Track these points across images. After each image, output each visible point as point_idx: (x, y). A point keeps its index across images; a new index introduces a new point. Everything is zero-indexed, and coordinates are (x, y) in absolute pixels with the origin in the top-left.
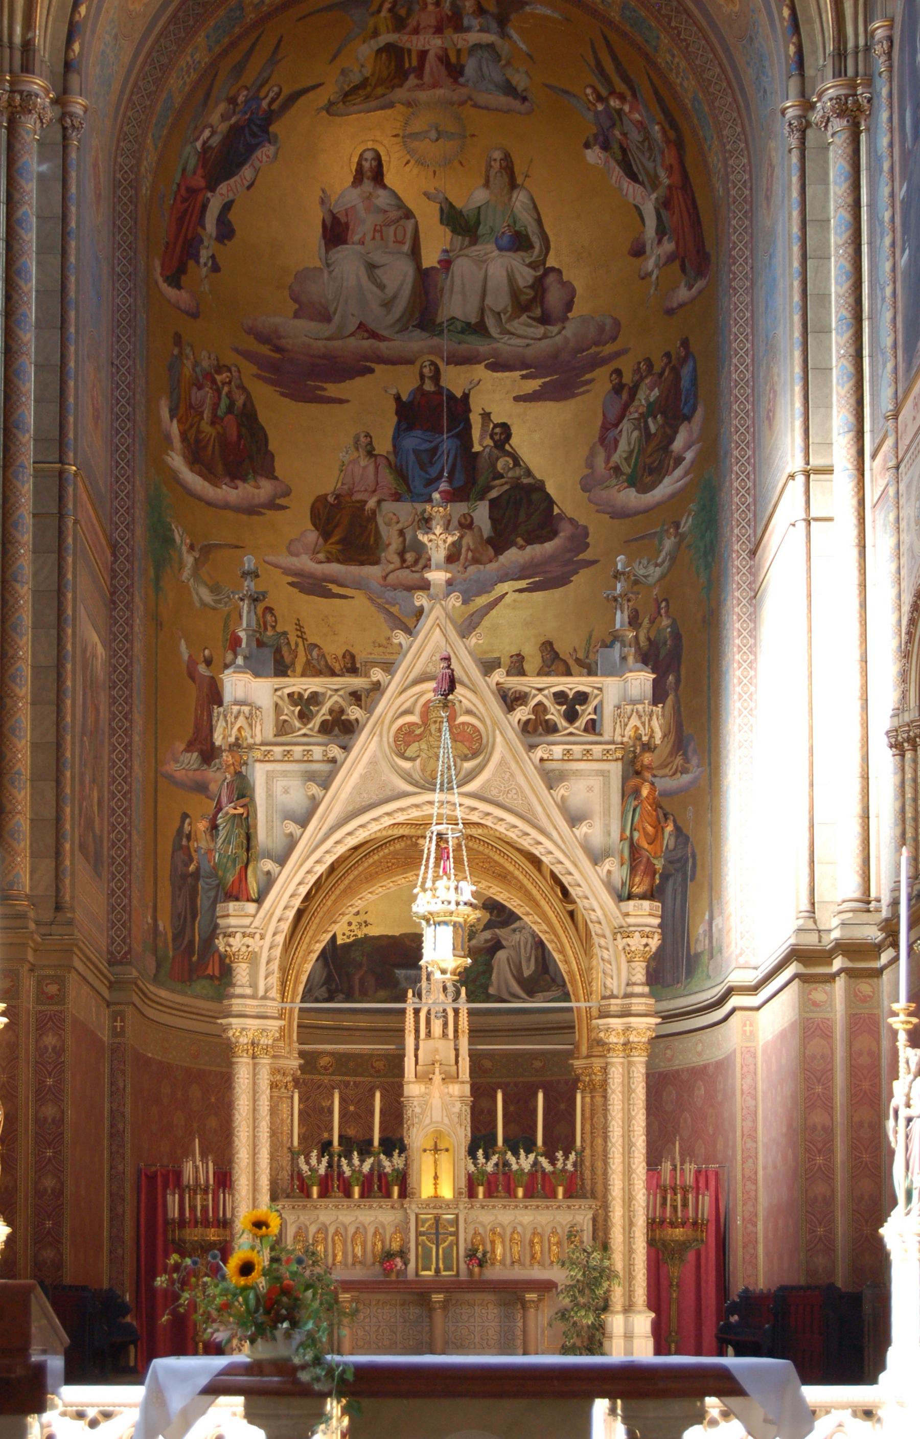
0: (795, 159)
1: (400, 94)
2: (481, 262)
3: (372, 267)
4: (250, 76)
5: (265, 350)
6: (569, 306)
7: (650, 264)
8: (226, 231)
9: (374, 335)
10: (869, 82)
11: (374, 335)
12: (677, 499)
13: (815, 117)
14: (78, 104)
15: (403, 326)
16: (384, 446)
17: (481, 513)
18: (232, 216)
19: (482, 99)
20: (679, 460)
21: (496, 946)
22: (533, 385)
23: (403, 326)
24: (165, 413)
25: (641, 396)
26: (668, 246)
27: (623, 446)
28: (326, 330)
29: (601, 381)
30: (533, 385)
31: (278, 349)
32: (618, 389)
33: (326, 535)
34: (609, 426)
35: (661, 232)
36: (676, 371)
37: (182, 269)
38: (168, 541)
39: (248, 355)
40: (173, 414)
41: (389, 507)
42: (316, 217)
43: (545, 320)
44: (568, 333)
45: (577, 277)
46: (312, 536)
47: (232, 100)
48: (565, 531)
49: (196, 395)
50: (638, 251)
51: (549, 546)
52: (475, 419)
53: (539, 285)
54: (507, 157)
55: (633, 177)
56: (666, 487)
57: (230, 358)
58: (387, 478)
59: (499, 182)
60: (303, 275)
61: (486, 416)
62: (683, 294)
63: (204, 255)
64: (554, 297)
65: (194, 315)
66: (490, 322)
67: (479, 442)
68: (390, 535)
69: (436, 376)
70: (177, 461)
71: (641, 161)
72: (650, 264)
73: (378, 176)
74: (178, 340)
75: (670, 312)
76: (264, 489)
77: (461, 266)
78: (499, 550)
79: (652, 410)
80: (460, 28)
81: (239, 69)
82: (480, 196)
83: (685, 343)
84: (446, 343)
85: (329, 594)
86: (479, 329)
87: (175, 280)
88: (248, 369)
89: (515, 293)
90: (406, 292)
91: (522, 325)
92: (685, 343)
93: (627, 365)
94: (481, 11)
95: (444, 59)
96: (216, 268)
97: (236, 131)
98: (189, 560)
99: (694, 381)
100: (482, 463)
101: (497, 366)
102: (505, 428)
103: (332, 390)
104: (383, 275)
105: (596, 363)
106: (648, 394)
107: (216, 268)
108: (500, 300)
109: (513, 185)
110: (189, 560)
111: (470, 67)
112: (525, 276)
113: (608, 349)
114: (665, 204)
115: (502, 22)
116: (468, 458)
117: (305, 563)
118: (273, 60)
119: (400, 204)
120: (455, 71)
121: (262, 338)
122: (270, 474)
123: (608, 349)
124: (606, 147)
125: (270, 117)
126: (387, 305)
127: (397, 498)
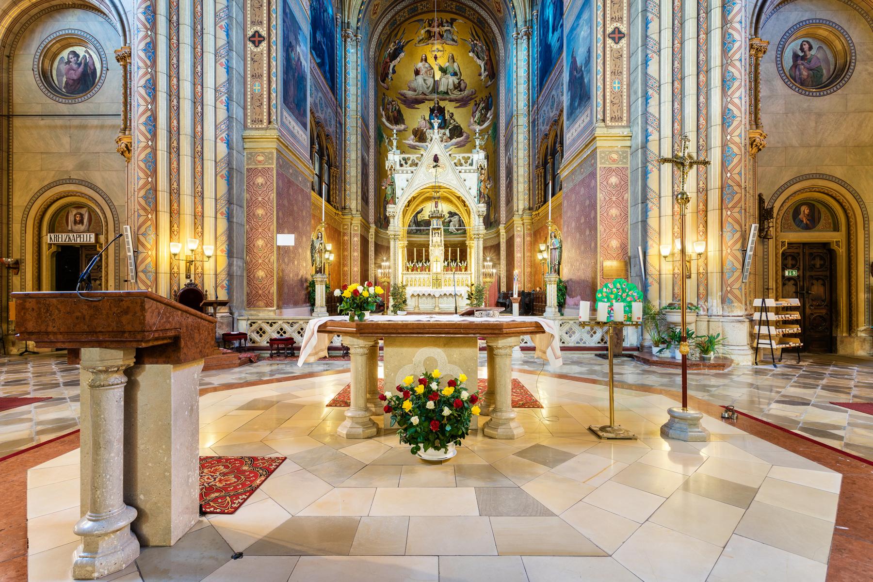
0: (515, 46)
1: (430, 42)
2: (447, 79)
3: (425, 80)
5: (402, 97)
6: (466, 87)
7: (483, 77)
8: (394, 72)
9: (425, 95)
10: (532, 27)
11: (425, 95)
12: (488, 127)
13: (520, 36)
15: (431, 92)
16: (427, 118)
17: (447, 132)
18: (395, 68)
19: (448, 42)
20: (488, 119)
21: (451, 221)
22: (458, 104)
23: (431, 92)
24: (381, 110)
25: (481, 106)
26: (486, 73)
27: (477, 117)
28: (416, 93)
29: (472, 103)
30: (458, 104)
31: (405, 97)
32: (476, 105)
33: (415, 136)
35: (485, 70)
36: (488, 100)
37: (385, 79)
38: (382, 137)
39: (399, 98)
40: (383, 110)
41: (428, 130)
43: (461, 91)
44: (466, 92)
45: (467, 81)
46: (412, 137)
47: (395, 42)
48: (465, 135)
49: (388, 106)
50: (480, 75)
51: (461, 138)
52: (446, 112)
53: (459, 83)
54: (453, 55)
55: (479, 58)
57: (395, 99)
58: (428, 125)
59: (451, 61)
60: (410, 82)
61: (448, 111)
62: (490, 83)
63: (390, 77)
64: (463, 86)
65: (388, 89)
66: (449, 91)
67: (447, 117)
68: (428, 136)
69: (438, 103)
70: (384, 120)
72: (483, 77)
73: (426, 60)
74: (384, 94)
75: (487, 87)
76: (402, 127)
77: (443, 79)
78: (451, 139)
79: (483, 108)
80: (443, 26)
81: (396, 35)
82: (447, 64)
83: (490, 94)
84: (441, 96)
85: (416, 149)
86: (447, 93)
87: (383, 81)
88: (399, 101)
89: (454, 85)
90: (432, 85)
91: (454, 92)
92: (490, 94)
93: (477, 99)
94: (447, 22)
95: (439, 33)
96: (392, 80)
97: (396, 49)
98: (387, 141)
99: (492, 102)
100: (448, 121)
101: (451, 101)
102: (452, 114)
103: (416, 106)
104: (427, 82)
105: (471, 99)
106: (482, 105)
107: (392, 80)
108: (451, 87)
109: (454, 62)
110: (387, 141)
111: (445, 35)
112: (456, 81)
113: (474, 96)
114: (486, 64)
116: (444, 120)
117: (411, 142)
118: (403, 33)
119: (430, 66)
120: (442, 36)
121: (402, 95)
122: (404, 124)
123: (474, 96)
124: (473, 52)
126: (428, 88)
127: (430, 129)
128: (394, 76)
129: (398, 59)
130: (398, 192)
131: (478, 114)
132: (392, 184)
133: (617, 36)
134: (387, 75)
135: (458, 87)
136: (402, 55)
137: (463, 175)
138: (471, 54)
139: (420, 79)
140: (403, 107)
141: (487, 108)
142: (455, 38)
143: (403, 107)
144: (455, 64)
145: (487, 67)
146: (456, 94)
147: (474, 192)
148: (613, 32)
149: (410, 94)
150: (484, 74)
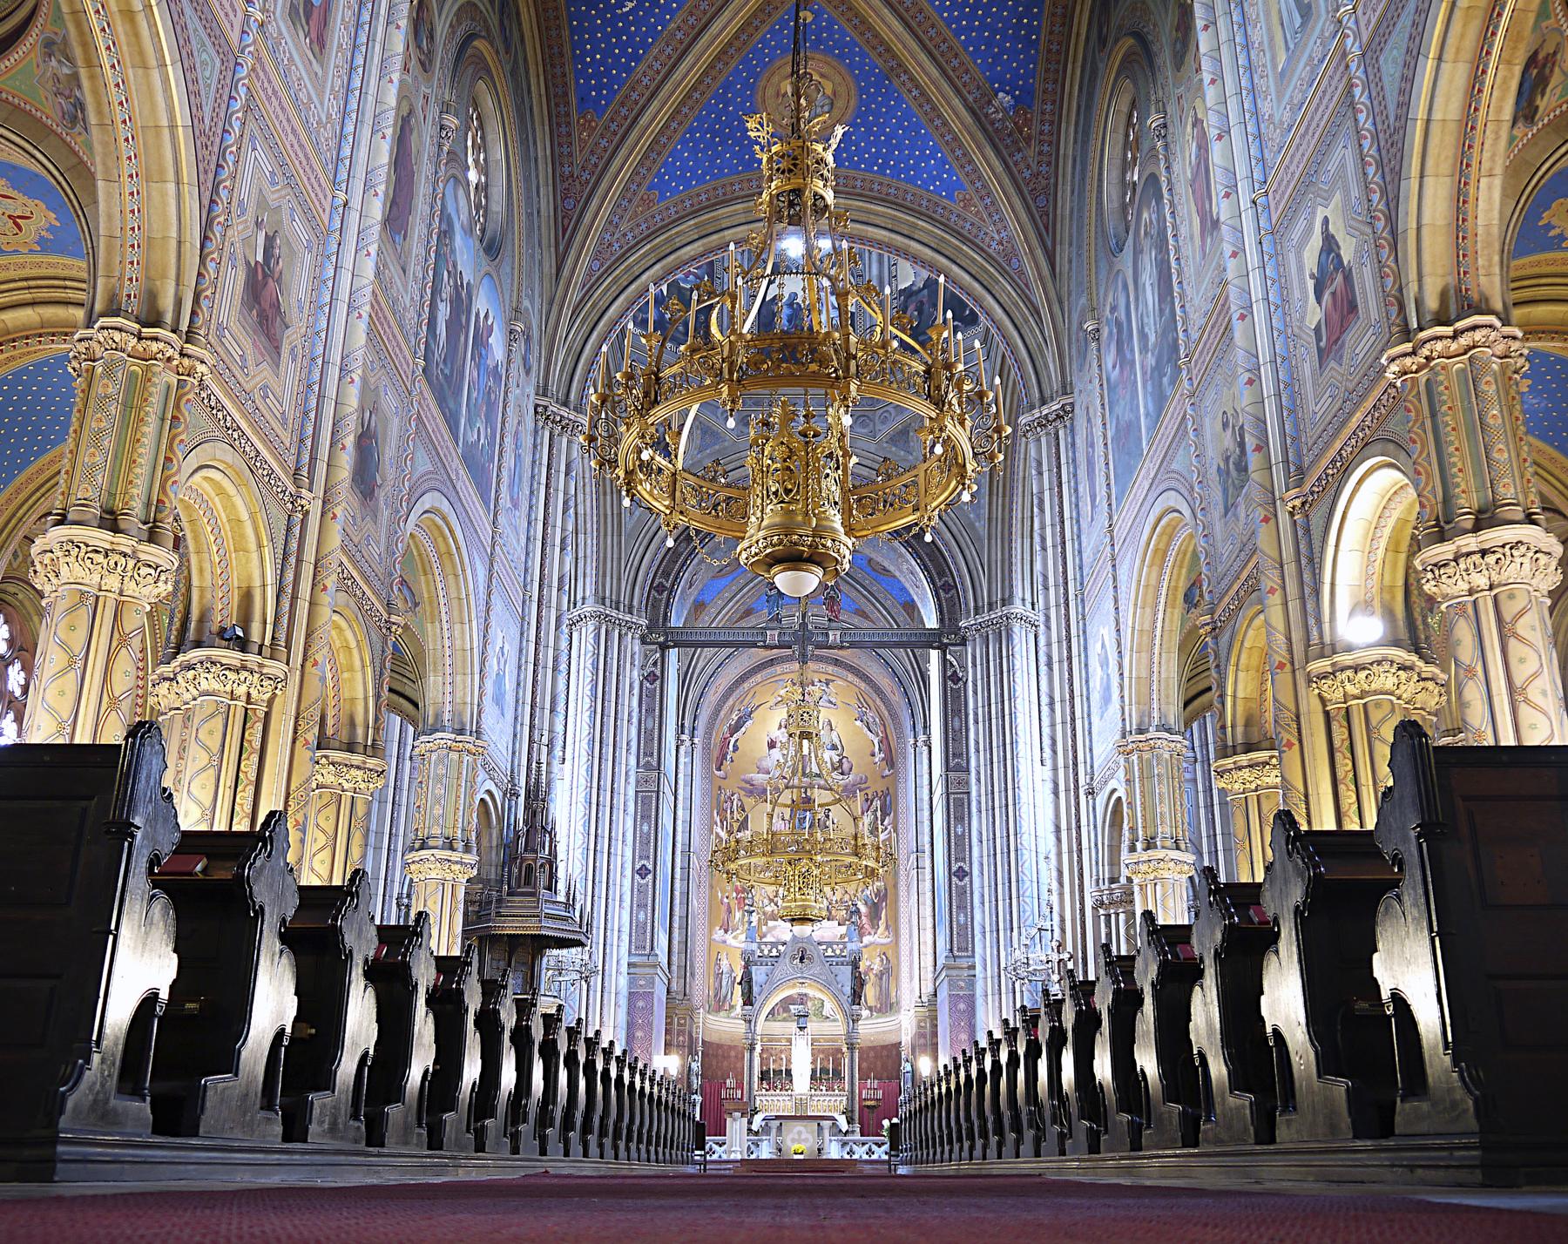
4: (745, 702)
8: (736, 748)
14: (696, 740)
32: (867, 800)
42: (767, 739)
43: (842, 774)
60: (760, 760)
64: (846, 766)
71: (873, 727)
74: (720, 788)
88: (742, 793)
89: (832, 764)
93: (870, 792)
115: (827, 684)
121: (747, 782)
125: (751, 712)
128: (735, 756)
129: (743, 729)
133: (961, 874)
134: (724, 757)
135: (838, 767)
138: (858, 723)
141: (885, 814)
142: (834, 700)
144: (834, 734)
145: (883, 748)
148: (958, 871)
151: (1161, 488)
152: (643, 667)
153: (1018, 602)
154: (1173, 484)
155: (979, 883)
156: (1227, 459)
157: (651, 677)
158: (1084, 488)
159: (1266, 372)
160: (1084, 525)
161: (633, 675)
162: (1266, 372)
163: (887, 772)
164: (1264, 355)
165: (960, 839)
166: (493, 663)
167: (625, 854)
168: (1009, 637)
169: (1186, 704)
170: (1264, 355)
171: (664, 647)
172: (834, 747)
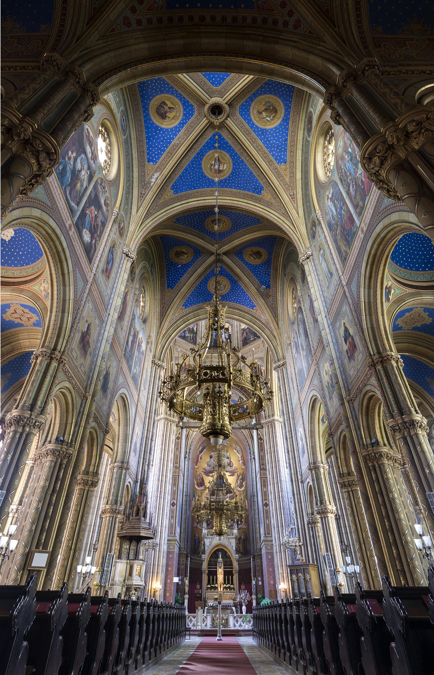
8: (201, 458)
34: (237, 480)
56: (243, 489)
62: (243, 467)
70: (196, 486)
79: (241, 479)
91: (228, 467)
106: (240, 477)
128: (201, 461)
130: (206, 548)
131: (239, 482)
132: (204, 544)
134: (198, 461)
136: (205, 450)
137: (230, 540)
139: (212, 459)
140: (204, 476)
141: (243, 481)
143: (204, 476)
146: (229, 468)
147: (234, 548)
149: (208, 468)
150: (241, 462)
151: (312, 389)
152: (176, 435)
153: (276, 415)
154: (315, 388)
155: (272, 508)
156: (328, 383)
157: (178, 438)
158: (291, 385)
159: (335, 361)
160: (292, 397)
161: (173, 437)
162: (335, 361)
163: (243, 467)
164: (334, 356)
165: (265, 493)
166: (135, 437)
167: (168, 498)
168: (275, 426)
169: (326, 452)
170: (334, 356)
171: (182, 428)
172: (228, 458)
